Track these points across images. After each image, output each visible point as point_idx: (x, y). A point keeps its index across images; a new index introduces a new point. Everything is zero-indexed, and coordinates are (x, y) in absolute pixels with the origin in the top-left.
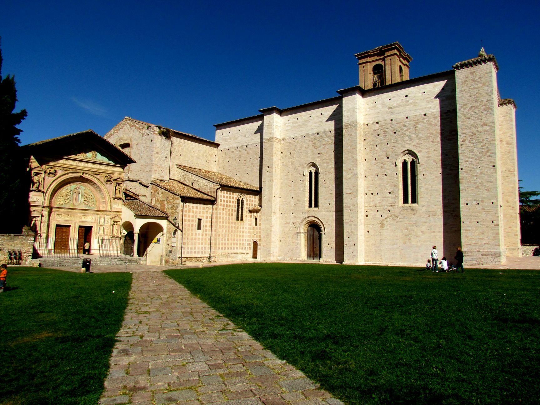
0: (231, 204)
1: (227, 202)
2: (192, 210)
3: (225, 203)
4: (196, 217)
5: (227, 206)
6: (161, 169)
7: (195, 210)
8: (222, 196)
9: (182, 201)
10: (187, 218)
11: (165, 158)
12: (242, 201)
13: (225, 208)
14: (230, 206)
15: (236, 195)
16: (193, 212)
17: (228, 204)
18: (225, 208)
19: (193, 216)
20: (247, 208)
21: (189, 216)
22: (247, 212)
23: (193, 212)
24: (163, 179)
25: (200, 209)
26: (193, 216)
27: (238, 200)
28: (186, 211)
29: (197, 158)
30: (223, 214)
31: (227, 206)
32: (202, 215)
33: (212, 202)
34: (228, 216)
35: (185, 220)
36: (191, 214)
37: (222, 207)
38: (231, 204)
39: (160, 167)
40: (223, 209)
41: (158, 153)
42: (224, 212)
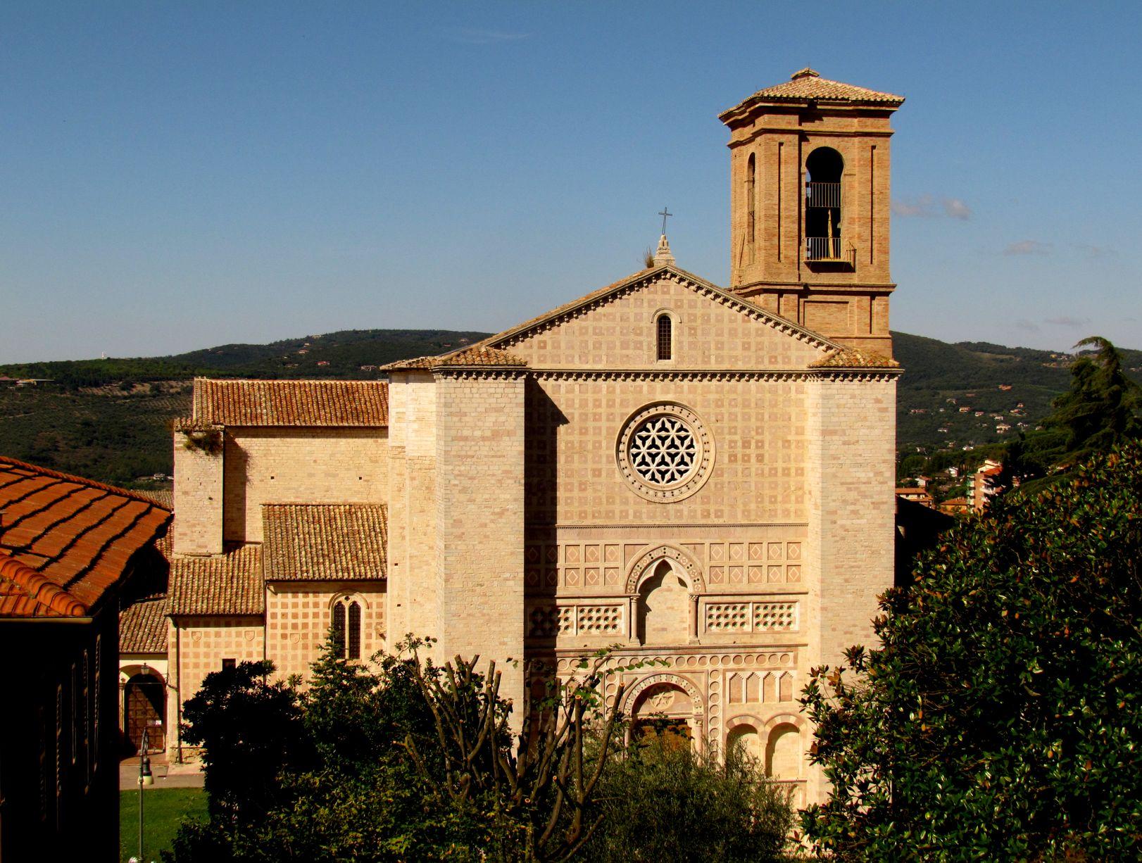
0: (310, 620)
1: (295, 616)
2: (203, 640)
3: (290, 621)
4: (216, 655)
5: (295, 626)
6: (198, 528)
7: (212, 639)
8: (277, 604)
9: (176, 625)
10: (191, 660)
11: (207, 502)
12: (355, 609)
13: (289, 631)
14: (305, 626)
15: (325, 599)
16: (208, 645)
17: (300, 621)
18: (289, 631)
19: (207, 655)
20: (369, 626)
21: (197, 655)
22: (369, 636)
23: (208, 645)
24: (204, 551)
25: (230, 635)
26: (207, 655)
27: (338, 610)
28: (187, 645)
29: (328, 475)
30: (284, 647)
31: (295, 626)
32: (234, 649)
33: (259, 619)
34: (300, 652)
35: (186, 666)
36: (202, 650)
37: (279, 631)
38: (310, 620)
39: (194, 525)
40: (284, 636)
41: (186, 493)
42: (289, 642)
